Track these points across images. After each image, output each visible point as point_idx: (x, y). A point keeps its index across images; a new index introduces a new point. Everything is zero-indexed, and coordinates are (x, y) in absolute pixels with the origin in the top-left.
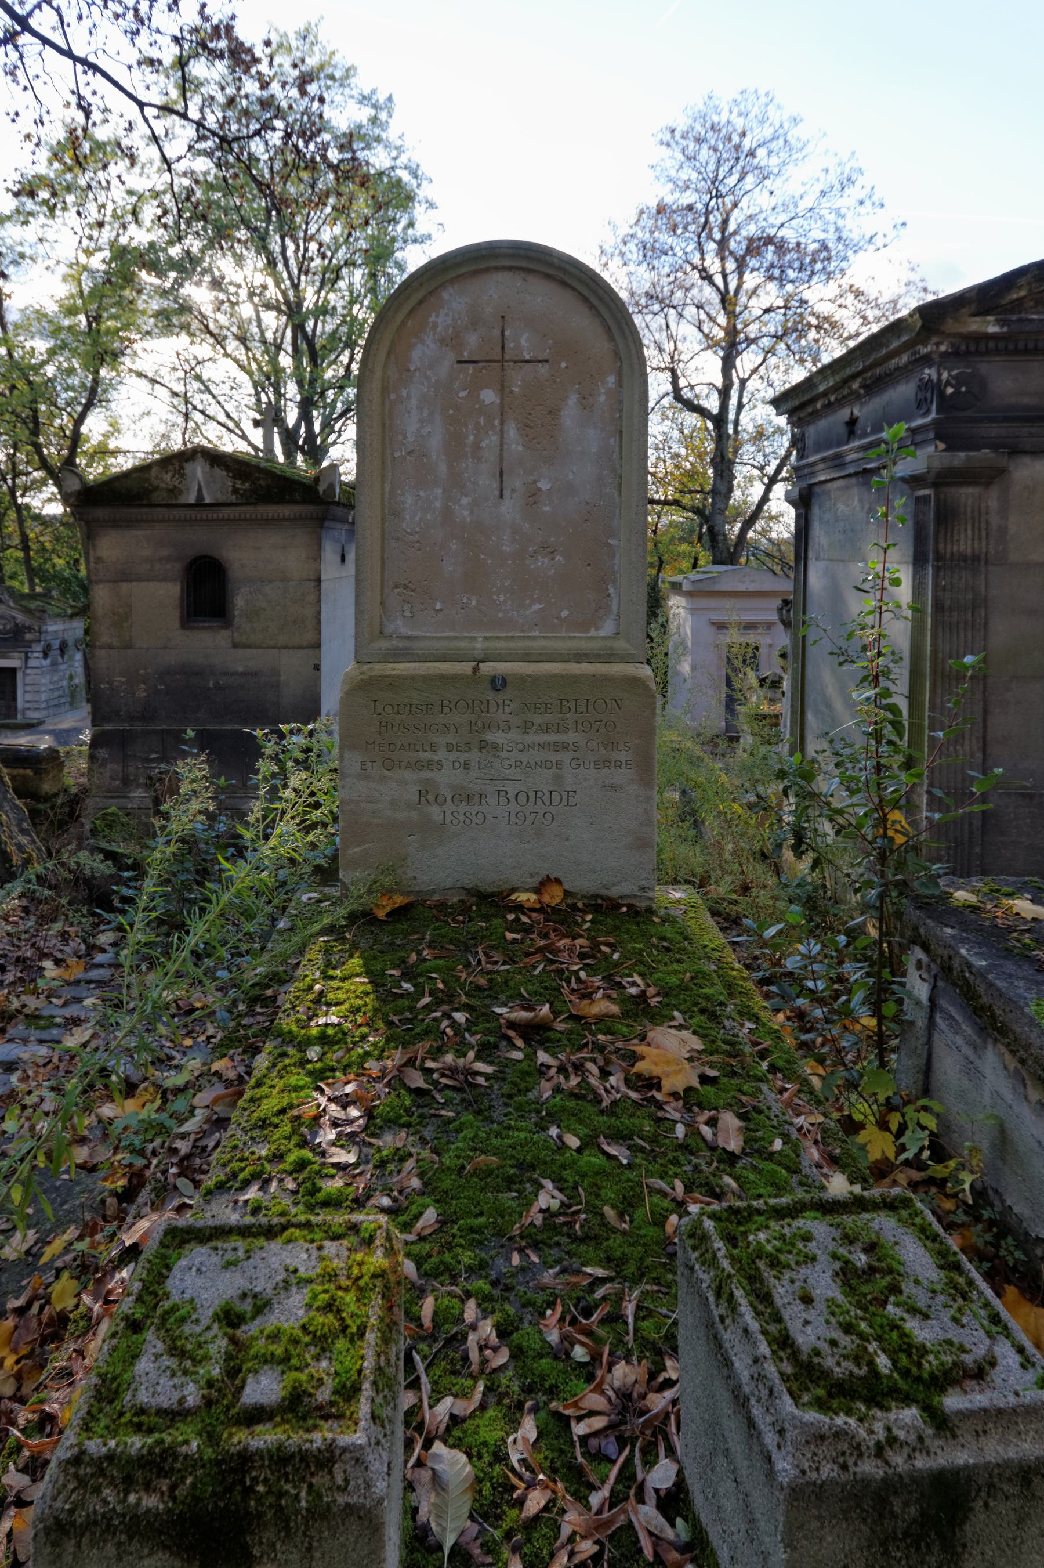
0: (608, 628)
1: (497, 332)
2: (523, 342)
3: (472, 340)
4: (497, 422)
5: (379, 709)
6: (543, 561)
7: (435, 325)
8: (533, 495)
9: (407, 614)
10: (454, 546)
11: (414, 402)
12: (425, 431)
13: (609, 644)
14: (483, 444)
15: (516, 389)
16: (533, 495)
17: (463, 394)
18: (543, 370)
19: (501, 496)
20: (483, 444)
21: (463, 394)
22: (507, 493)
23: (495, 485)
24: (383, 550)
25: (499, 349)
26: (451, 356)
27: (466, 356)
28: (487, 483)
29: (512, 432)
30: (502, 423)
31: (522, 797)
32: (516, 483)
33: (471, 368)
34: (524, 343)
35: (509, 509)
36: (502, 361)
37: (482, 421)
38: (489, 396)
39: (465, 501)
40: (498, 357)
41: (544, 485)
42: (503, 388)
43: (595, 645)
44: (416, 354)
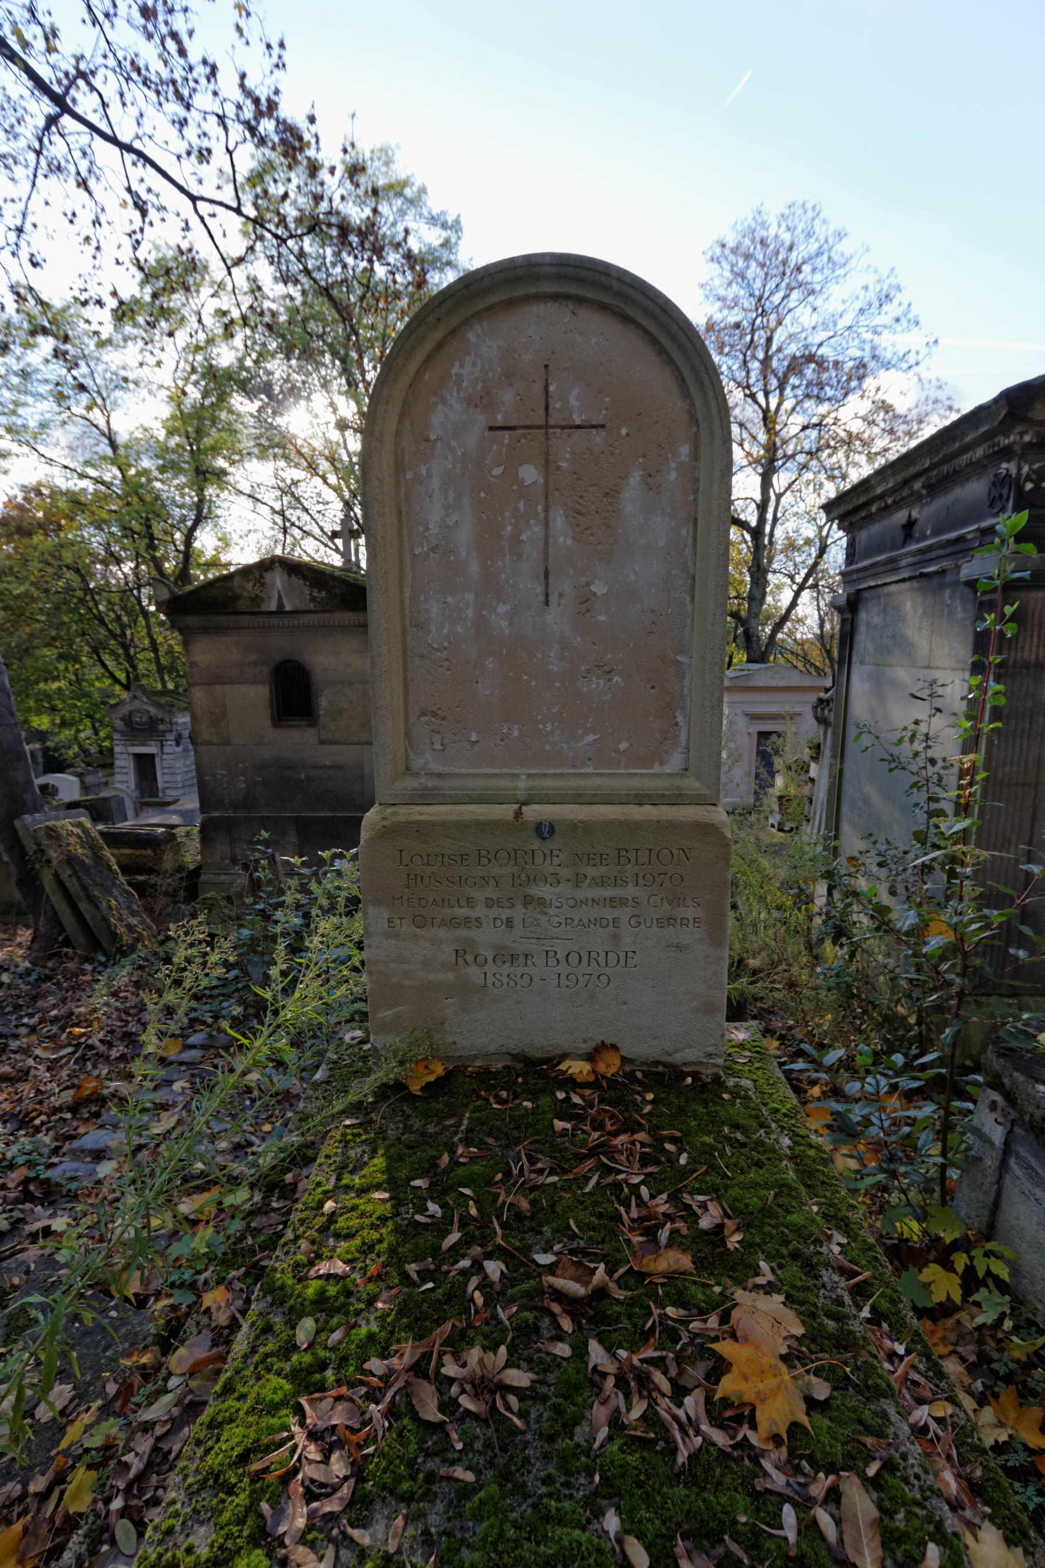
0: (674, 763)
1: (538, 388)
2: (573, 401)
3: (508, 397)
4: (540, 508)
5: (407, 861)
6: (598, 684)
7: (460, 379)
8: (586, 600)
10: (490, 664)
11: (436, 483)
12: (451, 521)
13: (677, 782)
14: (523, 537)
15: (564, 465)
16: (586, 600)
17: (497, 471)
18: (598, 438)
19: (547, 603)
20: (524, 537)
21: (497, 471)
22: (554, 599)
23: (540, 589)
24: (405, 669)
25: (541, 411)
26: (481, 419)
27: (500, 420)
28: (530, 586)
29: (559, 521)
30: (547, 510)
31: (574, 958)
32: (564, 585)
33: (507, 434)
34: (573, 401)
35: (557, 619)
37: (521, 506)
38: (530, 474)
39: (502, 609)
40: (541, 422)
41: (599, 588)
42: (547, 463)
44: (436, 419)
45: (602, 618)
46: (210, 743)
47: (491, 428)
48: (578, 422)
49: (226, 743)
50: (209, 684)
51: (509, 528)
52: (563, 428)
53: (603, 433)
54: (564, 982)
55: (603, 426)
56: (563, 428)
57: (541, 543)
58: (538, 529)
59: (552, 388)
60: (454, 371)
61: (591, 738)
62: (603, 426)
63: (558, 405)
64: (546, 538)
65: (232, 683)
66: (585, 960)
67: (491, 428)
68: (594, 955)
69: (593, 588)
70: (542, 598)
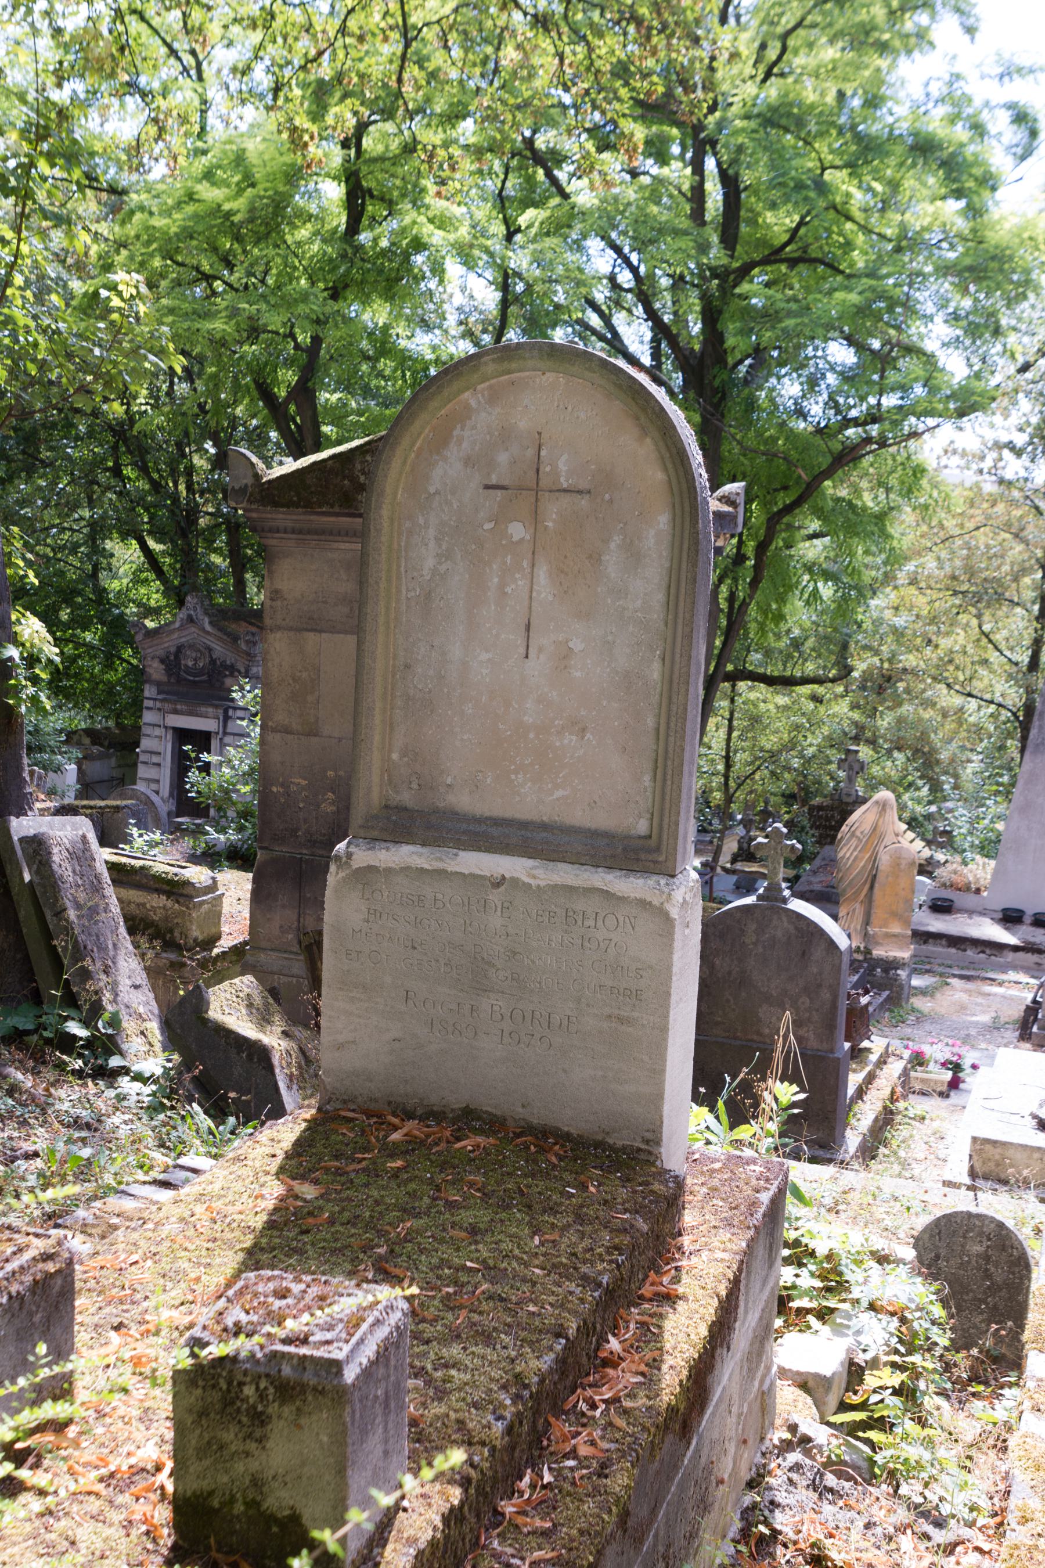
1: (530, 453)
2: (562, 466)
3: (503, 458)
4: (525, 564)
7: (460, 440)
8: (564, 656)
11: (432, 532)
12: (443, 568)
14: (509, 590)
15: (550, 524)
16: (564, 656)
17: (488, 526)
18: (584, 502)
20: (509, 590)
21: (488, 526)
23: (521, 642)
25: (532, 474)
27: (494, 480)
29: (542, 574)
33: (499, 493)
34: (562, 467)
37: (508, 559)
38: (517, 531)
39: (484, 656)
41: (576, 645)
42: (536, 517)
44: (437, 473)
45: (578, 674)
46: (287, 731)
47: (487, 487)
48: (565, 485)
49: (313, 732)
50: (299, 630)
54: (506, 1039)
59: (543, 453)
65: (333, 630)
67: (487, 487)
68: (537, 1014)
69: (571, 644)
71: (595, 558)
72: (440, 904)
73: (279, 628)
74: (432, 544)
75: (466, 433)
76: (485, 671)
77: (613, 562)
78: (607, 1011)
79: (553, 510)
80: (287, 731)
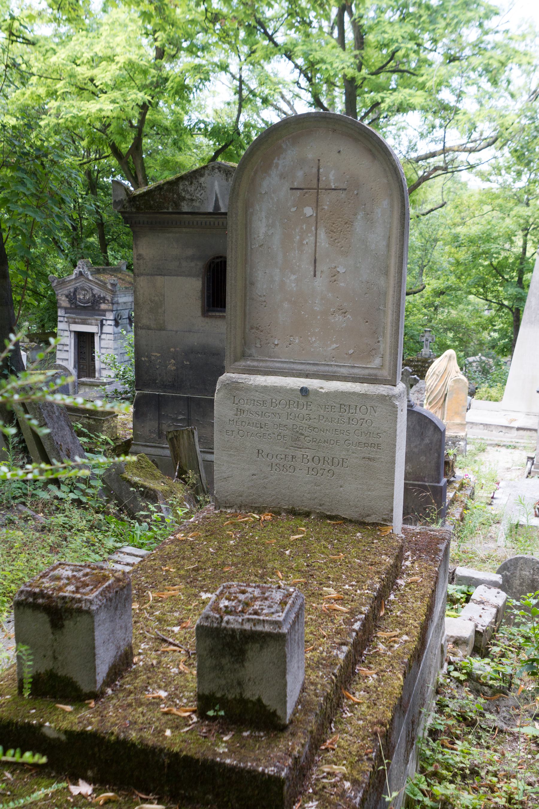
0: (377, 361)
1: (315, 170)
2: (331, 177)
3: (300, 174)
4: (313, 228)
6: (338, 318)
7: (277, 166)
8: (334, 275)
9: (258, 345)
10: (286, 305)
11: (264, 214)
12: (270, 233)
14: (305, 242)
16: (334, 275)
17: (293, 209)
18: (343, 195)
19: (315, 276)
20: (305, 242)
21: (293, 209)
23: (312, 268)
25: (315, 181)
26: (286, 186)
27: (296, 185)
28: (306, 266)
29: (322, 235)
30: (316, 229)
32: (322, 267)
33: (298, 192)
34: (331, 177)
35: (320, 283)
36: (318, 188)
38: (309, 211)
39: (293, 277)
40: (315, 186)
41: (341, 270)
42: (317, 205)
43: (366, 372)
44: (265, 184)
45: (342, 284)
46: (149, 328)
47: (291, 189)
48: (333, 187)
49: (162, 328)
50: (152, 275)
51: (298, 237)
52: (326, 189)
53: (345, 192)
55: (345, 189)
56: (326, 189)
57: (313, 245)
58: (312, 239)
59: (321, 170)
60: (275, 161)
61: (335, 346)
62: (345, 189)
63: (324, 178)
64: (316, 243)
65: (170, 274)
66: (322, 461)
67: (291, 189)
68: (326, 459)
69: (338, 269)
70: (312, 273)
71: (349, 223)
72: (274, 405)
73: (142, 274)
74: (264, 220)
75: (280, 162)
76: (293, 285)
77: (359, 225)
78: (363, 455)
79: (327, 200)
80: (149, 328)
